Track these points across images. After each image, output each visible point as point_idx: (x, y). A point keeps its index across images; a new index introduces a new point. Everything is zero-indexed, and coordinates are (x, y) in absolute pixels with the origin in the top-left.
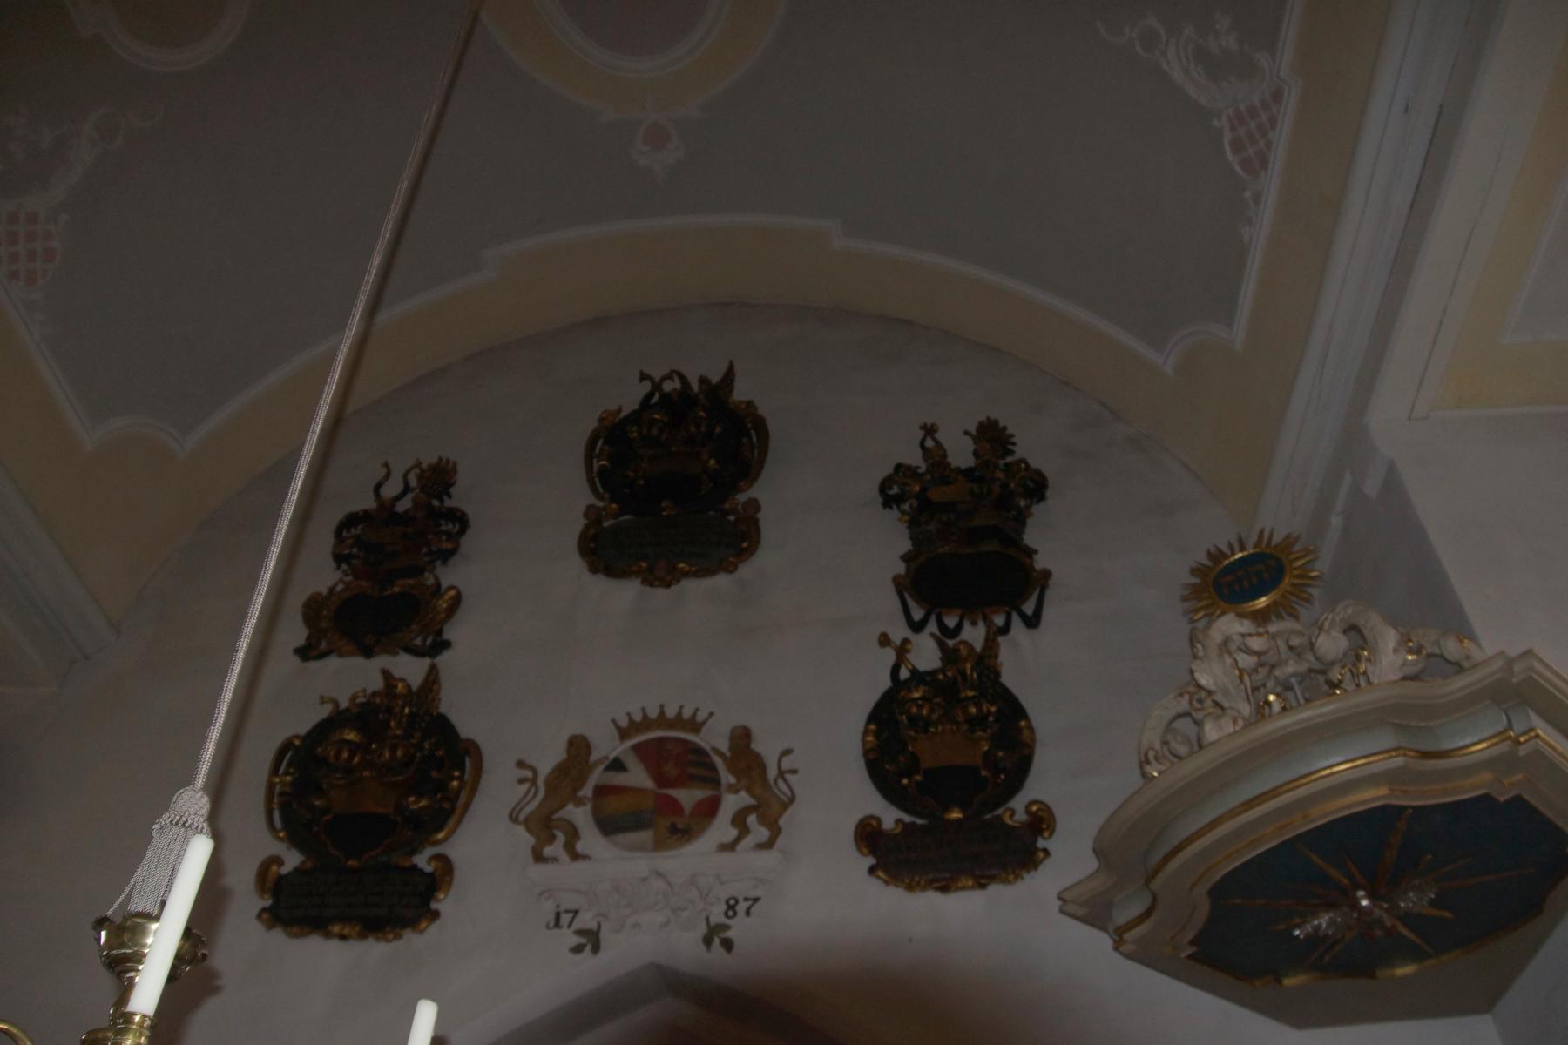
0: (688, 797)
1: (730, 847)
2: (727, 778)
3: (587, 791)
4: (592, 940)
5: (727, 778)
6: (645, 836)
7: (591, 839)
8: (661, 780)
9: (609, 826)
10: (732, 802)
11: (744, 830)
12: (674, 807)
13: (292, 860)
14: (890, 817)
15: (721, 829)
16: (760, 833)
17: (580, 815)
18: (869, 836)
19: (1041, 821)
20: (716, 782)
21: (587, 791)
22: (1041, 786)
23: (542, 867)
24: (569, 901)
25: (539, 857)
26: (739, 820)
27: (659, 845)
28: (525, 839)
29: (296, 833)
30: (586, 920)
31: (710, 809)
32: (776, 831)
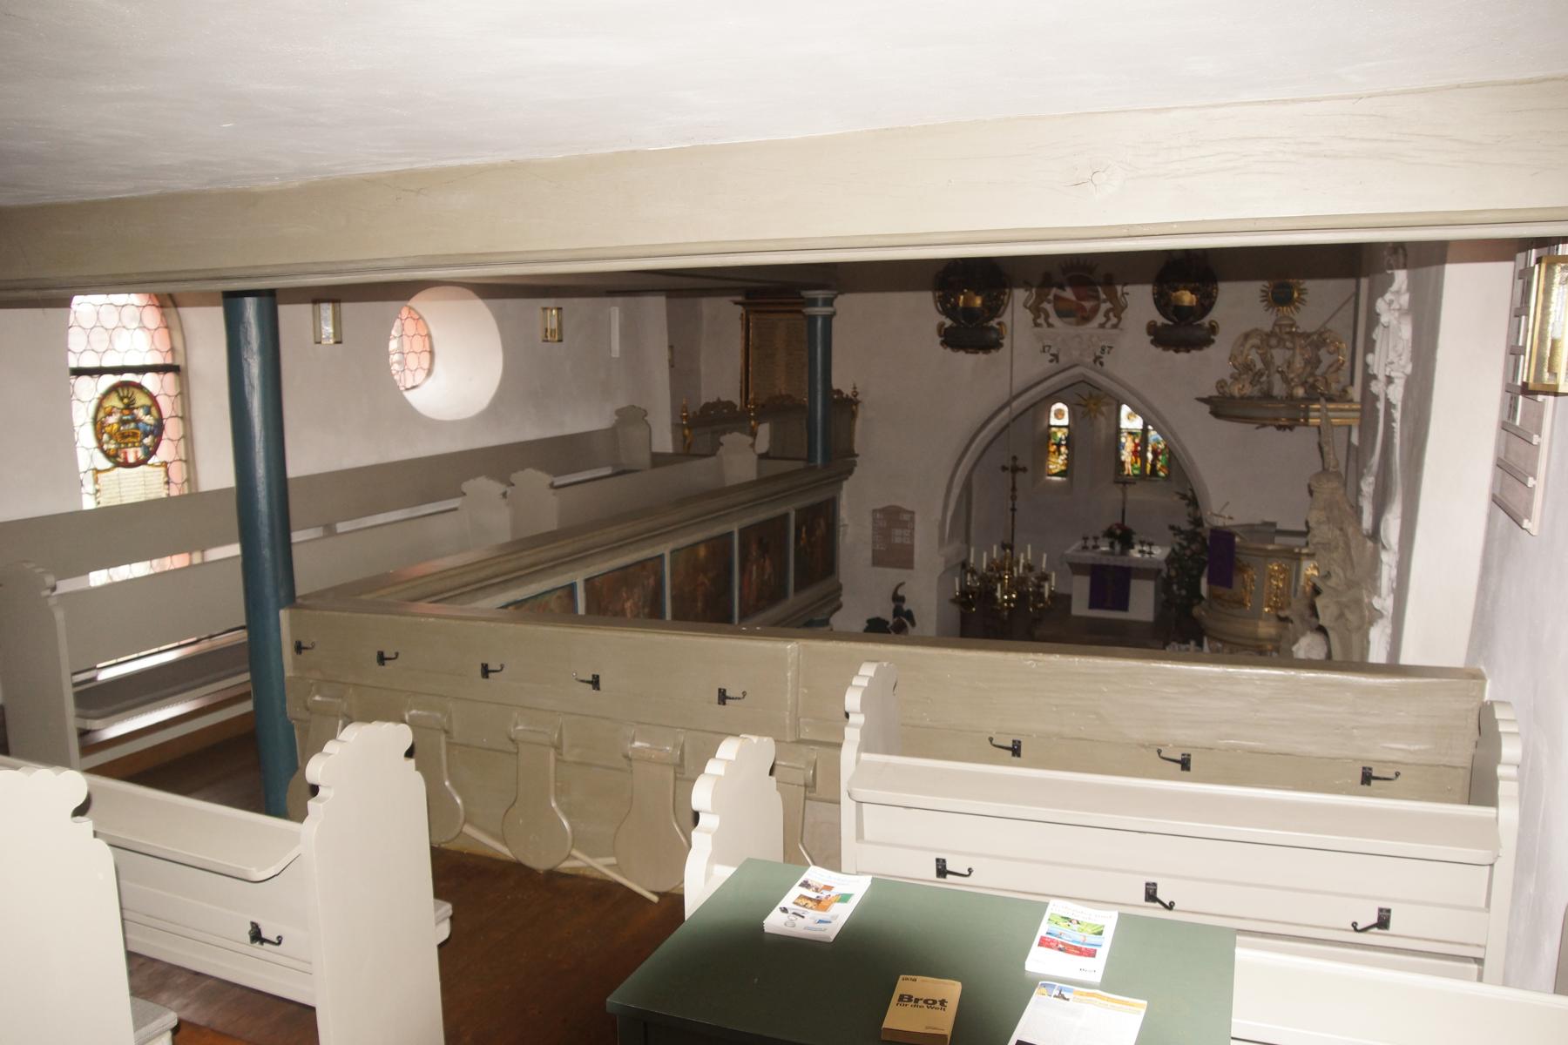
0: (1088, 305)
1: (1102, 326)
2: (1103, 296)
3: (1051, 297)
4: (1055, 358)
5: (1103, 296)
6: (1072, 320)
7: (1054, 319)
8: (1079, 298)
9: (1061, 314)
10: (1105, 306)
11: (1108, 319)
12: (1083, 308)
13: (948, 322)
14: (1161, 320)
15: (1100, 318)
16: (1114, 320)
17: (1049, 307)
18: (1152, 329)
19: (1213, 329)
20: (1097, 298)
21: (1051, 297)
22: (1215, 315)
23: (1037, 329)
24: (1048, 342)
25: (1037, 325)
26: (1106, 315)
27: (1078, 324)
28: (1029, 316)
29: (945, 312)
30: (1053, 351)
31: (1095, 310)
32: (1120, 319)
